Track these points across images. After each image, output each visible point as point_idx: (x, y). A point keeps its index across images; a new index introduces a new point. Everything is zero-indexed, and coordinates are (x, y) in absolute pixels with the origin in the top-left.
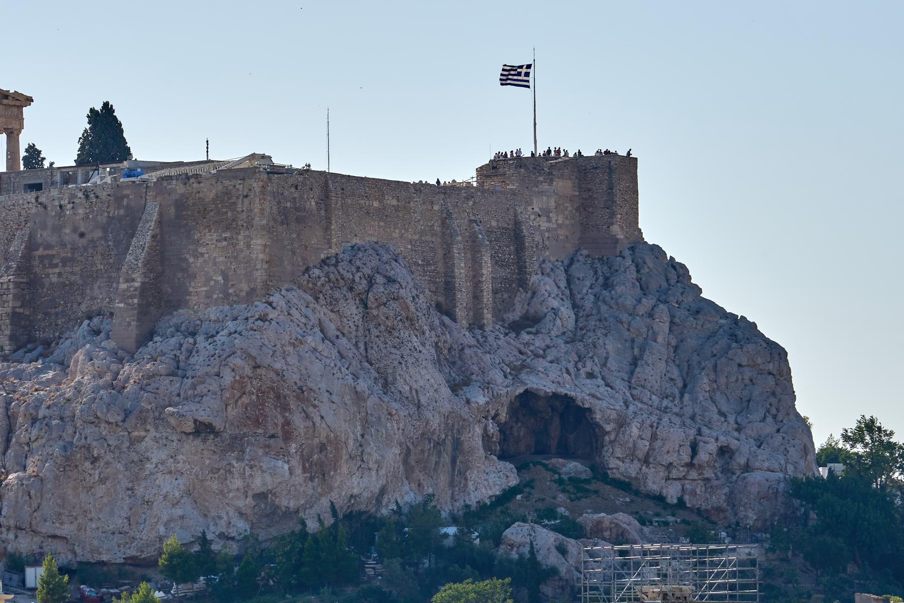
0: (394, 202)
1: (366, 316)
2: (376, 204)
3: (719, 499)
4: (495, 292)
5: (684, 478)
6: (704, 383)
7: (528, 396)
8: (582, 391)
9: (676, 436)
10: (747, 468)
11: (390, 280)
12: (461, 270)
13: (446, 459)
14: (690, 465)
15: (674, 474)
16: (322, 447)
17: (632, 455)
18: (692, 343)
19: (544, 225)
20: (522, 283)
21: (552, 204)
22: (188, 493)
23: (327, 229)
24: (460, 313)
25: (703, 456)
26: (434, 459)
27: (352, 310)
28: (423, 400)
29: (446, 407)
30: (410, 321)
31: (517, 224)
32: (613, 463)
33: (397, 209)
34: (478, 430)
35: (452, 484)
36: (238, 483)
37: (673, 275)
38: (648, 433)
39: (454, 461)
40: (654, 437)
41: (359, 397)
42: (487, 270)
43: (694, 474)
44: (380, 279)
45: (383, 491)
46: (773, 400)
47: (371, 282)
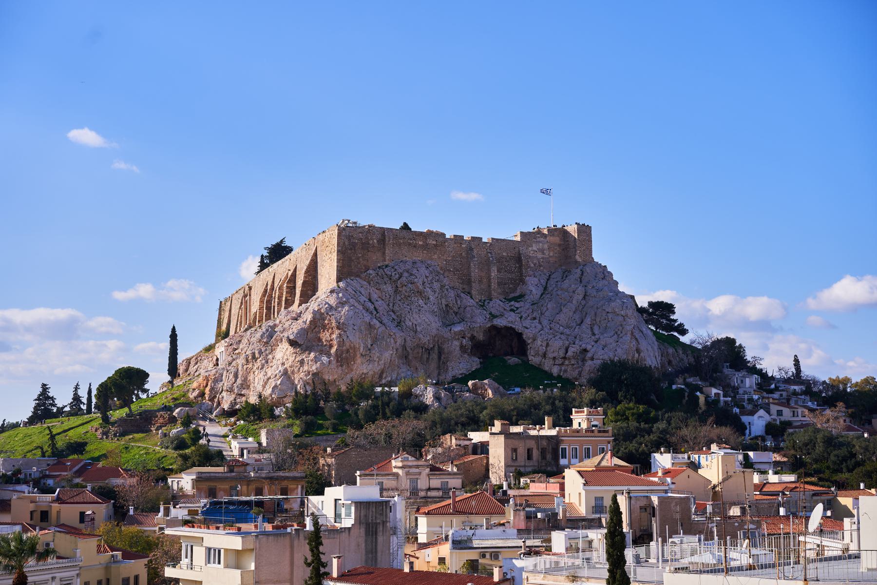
0: (434, 242)
1: (396, 291)
2: (421, 243)
3: (575, 374)
4: (499, 284)
5: (562, 364)
6: (588, 321)
7: (494, 328)
8: (518, 327)
9: (557, 344)
10: (592, 359)
11: (411, 275)
12: (475, 272)
13: (435, 356)
14: (565, 358)
15: (557, 362)
16: (348, 351)
17: (537, 354)
18: (591, 303)
19: (540, 255)
20: (522, 281)
21: (546, 246)
22: (285, 373)
23: (384, 253)
24: (473, 292)
25: (570, 353)
26: (425, 356)
27: (389, 288)
28: (419, 329)
29: (434, 332)
30: (420, 293)
31: (520, 254)
32: (530, 358)
33: (436, 246)
34: (457, 343)
35: (439, 368)
36: (306, 368)
37: (601, 276)
38: (544, 344)
39: (439, 358)
40: (547, 345)
41: (370, 326)
42: (494, 273)
43: (567, 362)
44: (406, 274)
45: (382, 373)
46: (620, 328)
47: (400, 277)
